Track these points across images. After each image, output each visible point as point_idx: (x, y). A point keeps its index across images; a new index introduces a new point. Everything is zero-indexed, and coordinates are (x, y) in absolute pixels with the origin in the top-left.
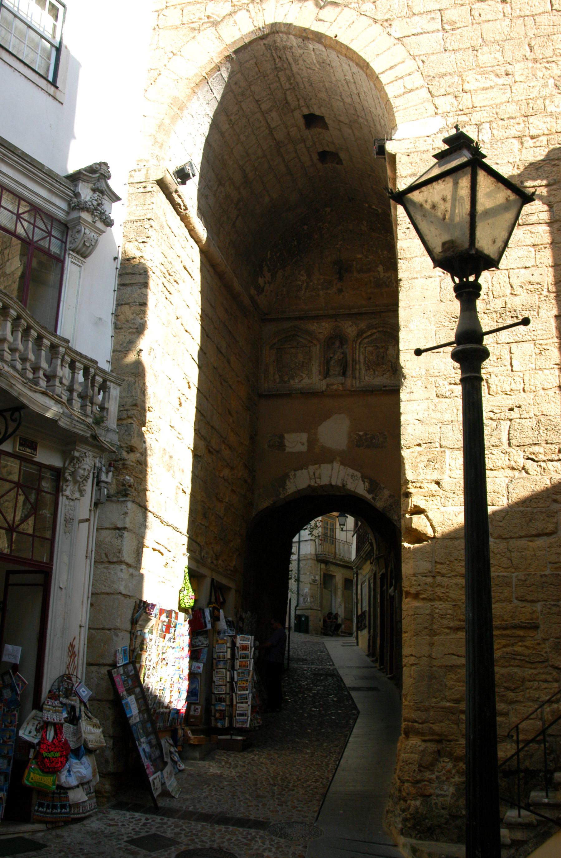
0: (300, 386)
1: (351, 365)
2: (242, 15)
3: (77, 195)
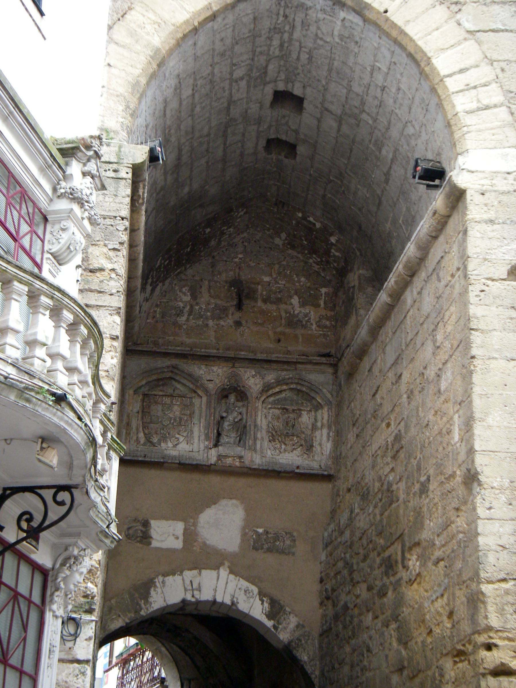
0: (174, 453)
1: (252, 432)
3: (66, 177)
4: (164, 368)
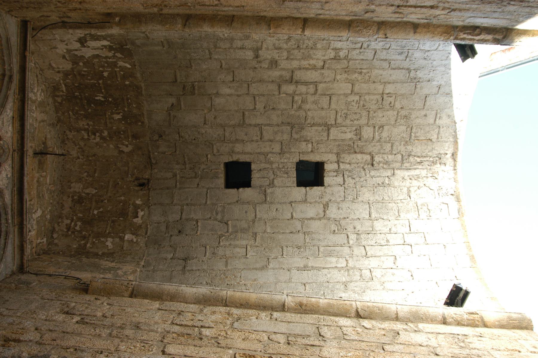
4: (10, 65)
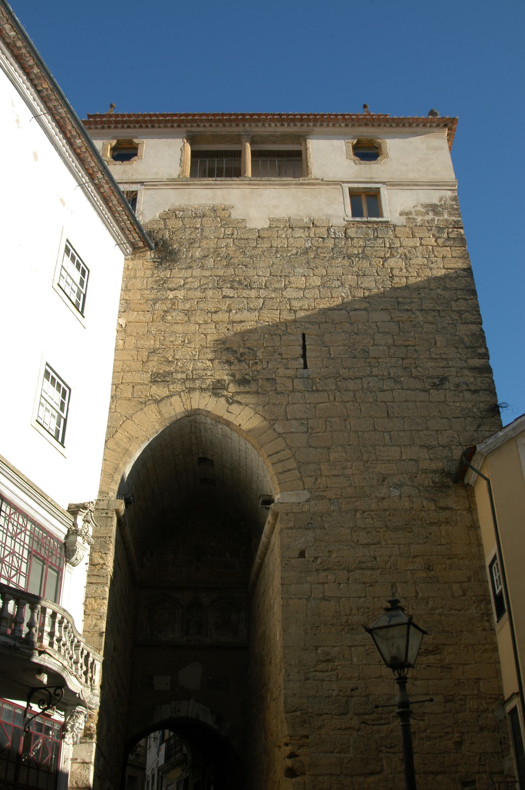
2: (175, 399)
